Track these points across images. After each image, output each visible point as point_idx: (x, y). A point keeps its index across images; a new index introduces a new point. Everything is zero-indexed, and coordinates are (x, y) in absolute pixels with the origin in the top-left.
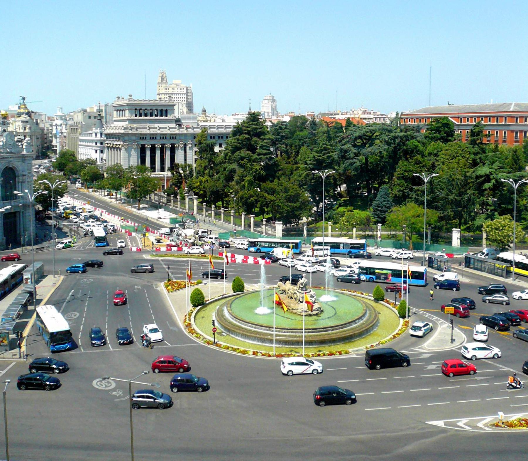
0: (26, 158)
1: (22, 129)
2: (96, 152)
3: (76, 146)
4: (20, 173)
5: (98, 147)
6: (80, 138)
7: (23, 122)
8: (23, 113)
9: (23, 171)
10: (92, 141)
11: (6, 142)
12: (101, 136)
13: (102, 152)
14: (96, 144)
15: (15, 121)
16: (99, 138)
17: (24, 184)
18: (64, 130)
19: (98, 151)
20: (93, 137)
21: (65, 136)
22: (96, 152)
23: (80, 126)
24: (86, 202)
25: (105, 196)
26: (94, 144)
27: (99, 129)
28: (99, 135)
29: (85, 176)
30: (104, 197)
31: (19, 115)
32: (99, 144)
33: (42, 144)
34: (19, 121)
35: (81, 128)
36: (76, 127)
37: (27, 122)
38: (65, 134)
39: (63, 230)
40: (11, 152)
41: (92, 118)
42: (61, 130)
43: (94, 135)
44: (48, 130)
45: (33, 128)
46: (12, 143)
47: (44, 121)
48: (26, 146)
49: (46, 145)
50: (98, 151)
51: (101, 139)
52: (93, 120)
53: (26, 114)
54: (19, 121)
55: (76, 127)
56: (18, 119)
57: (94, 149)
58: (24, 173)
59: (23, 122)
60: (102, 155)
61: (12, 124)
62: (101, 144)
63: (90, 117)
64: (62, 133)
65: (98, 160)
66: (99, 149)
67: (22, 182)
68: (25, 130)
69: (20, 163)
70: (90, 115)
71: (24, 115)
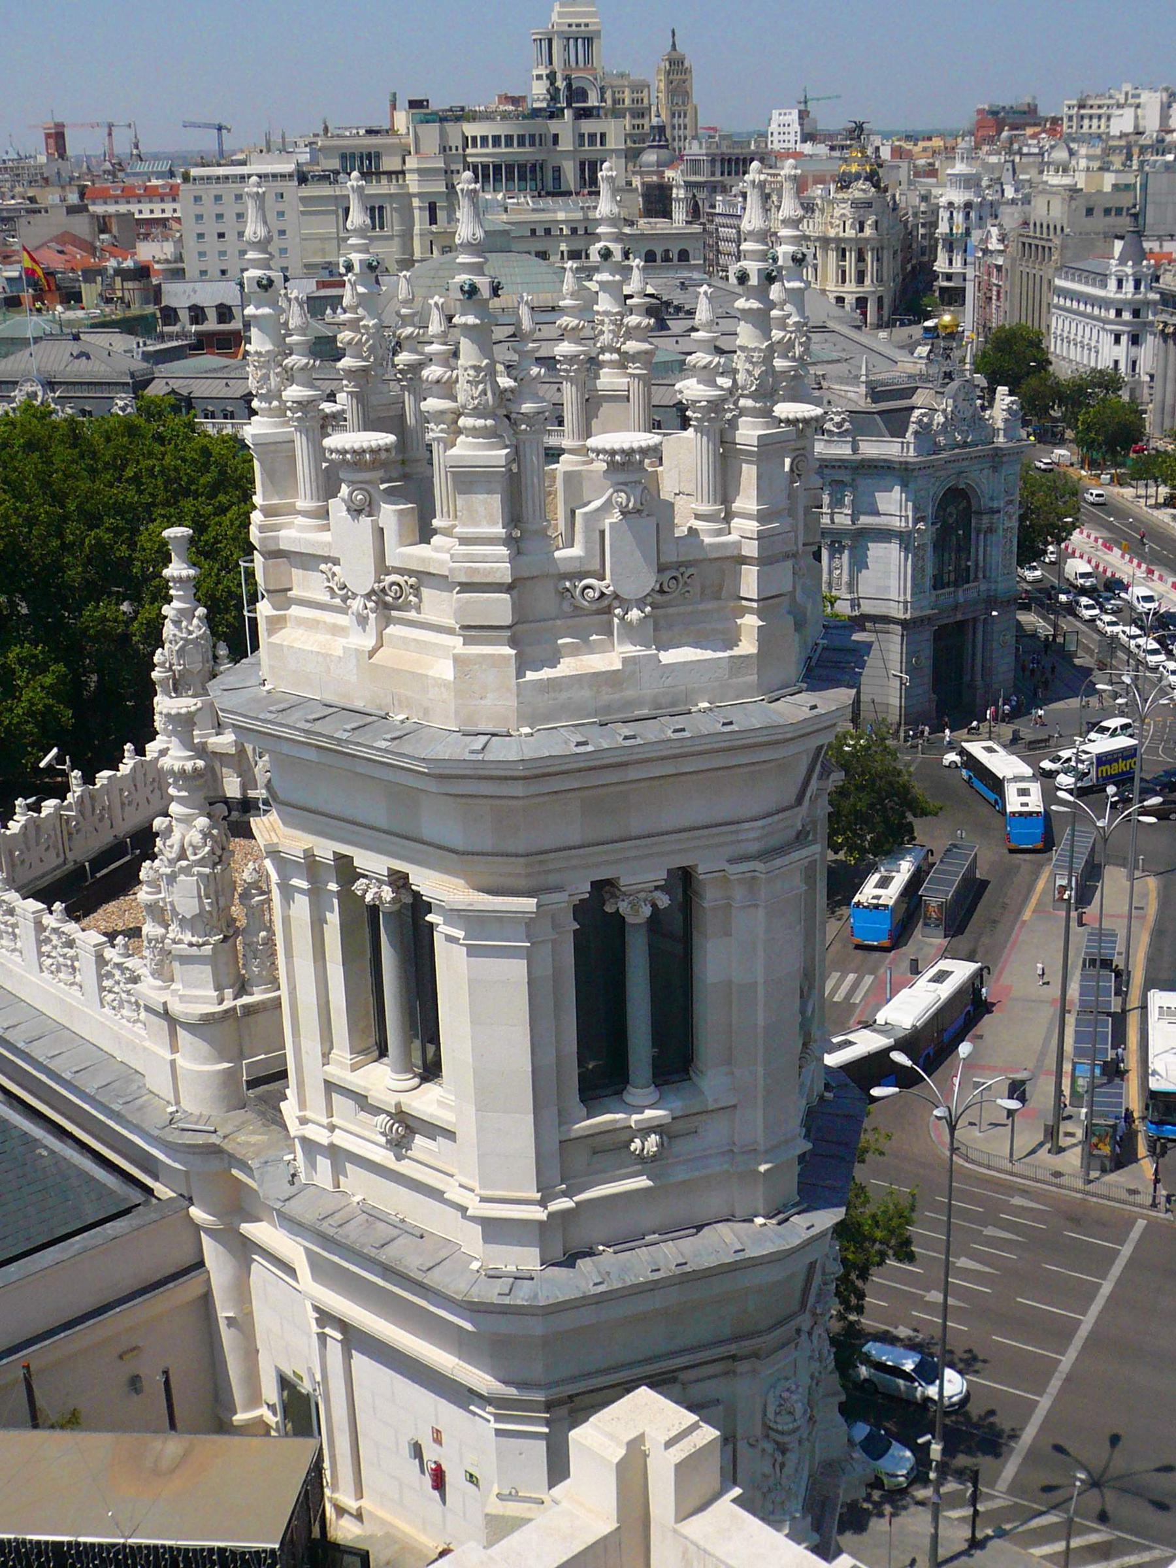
0: (1005, 459)
1: (852, 226)
2: (1117, 340)
3: (1040, 308)
4: (985, 502)
5: (1125, 323)
6: (1059, 282)
7: (856, 204)
8: (857, 177)
9: (992, 499)
10: (1104, 303)
11: (952, 412)
12: (1137, 286)
13: (1135, 340)
14: (1119, 313)
15: (831, 202)
16: (1129, 296)
17: (994, 538)
18: (994, 245)
19: (1124, 339)
20: (1111, 291)
21: (999, 268)
22: (1117, 340)
23: (1057, 241)
24: (1106, 535)
25: (1157, 506)
26: (1112, 314)
27: (1130, 263)
28: (1129, 286)
29: (1088, 429)
30: (1156, 513)
31: (845, 182)
32: (1127, 316)
33: (903, 268)
34: (844, 201)
35: (1064, 247)
36: (1043, 243)
37: (869, 205)
38: (1000, 262)
39: (1077, 661)
40: (965, 444)
41: (1098, 213)
42: (985, 240)
43: (1112, 283)
44: (915, 215)
45: (884, 225)
46: (968, 415)
47: (904, 186)
48: (1006, 421)
49: (909, 267)
50: (1124, 339)
51: (1137, 296)
52: (1100, 222)
53: (866, 179)
54: (844, 201)
55: (1043, 243)
56: (840, 196)
57: (1111, 331)
58: (995, 505)
59: (856, 204)
60: (1133, 350)
61: (822, 211)
62: (1136, 313)
63: (1090, 212)
64: (986, 251)
65: (1122, 366)
66: (1129, 333)
67: (991, 530)
68: (862, 230)
69: (985, 472)
70: (1091, 205)
71: (860, 184)
